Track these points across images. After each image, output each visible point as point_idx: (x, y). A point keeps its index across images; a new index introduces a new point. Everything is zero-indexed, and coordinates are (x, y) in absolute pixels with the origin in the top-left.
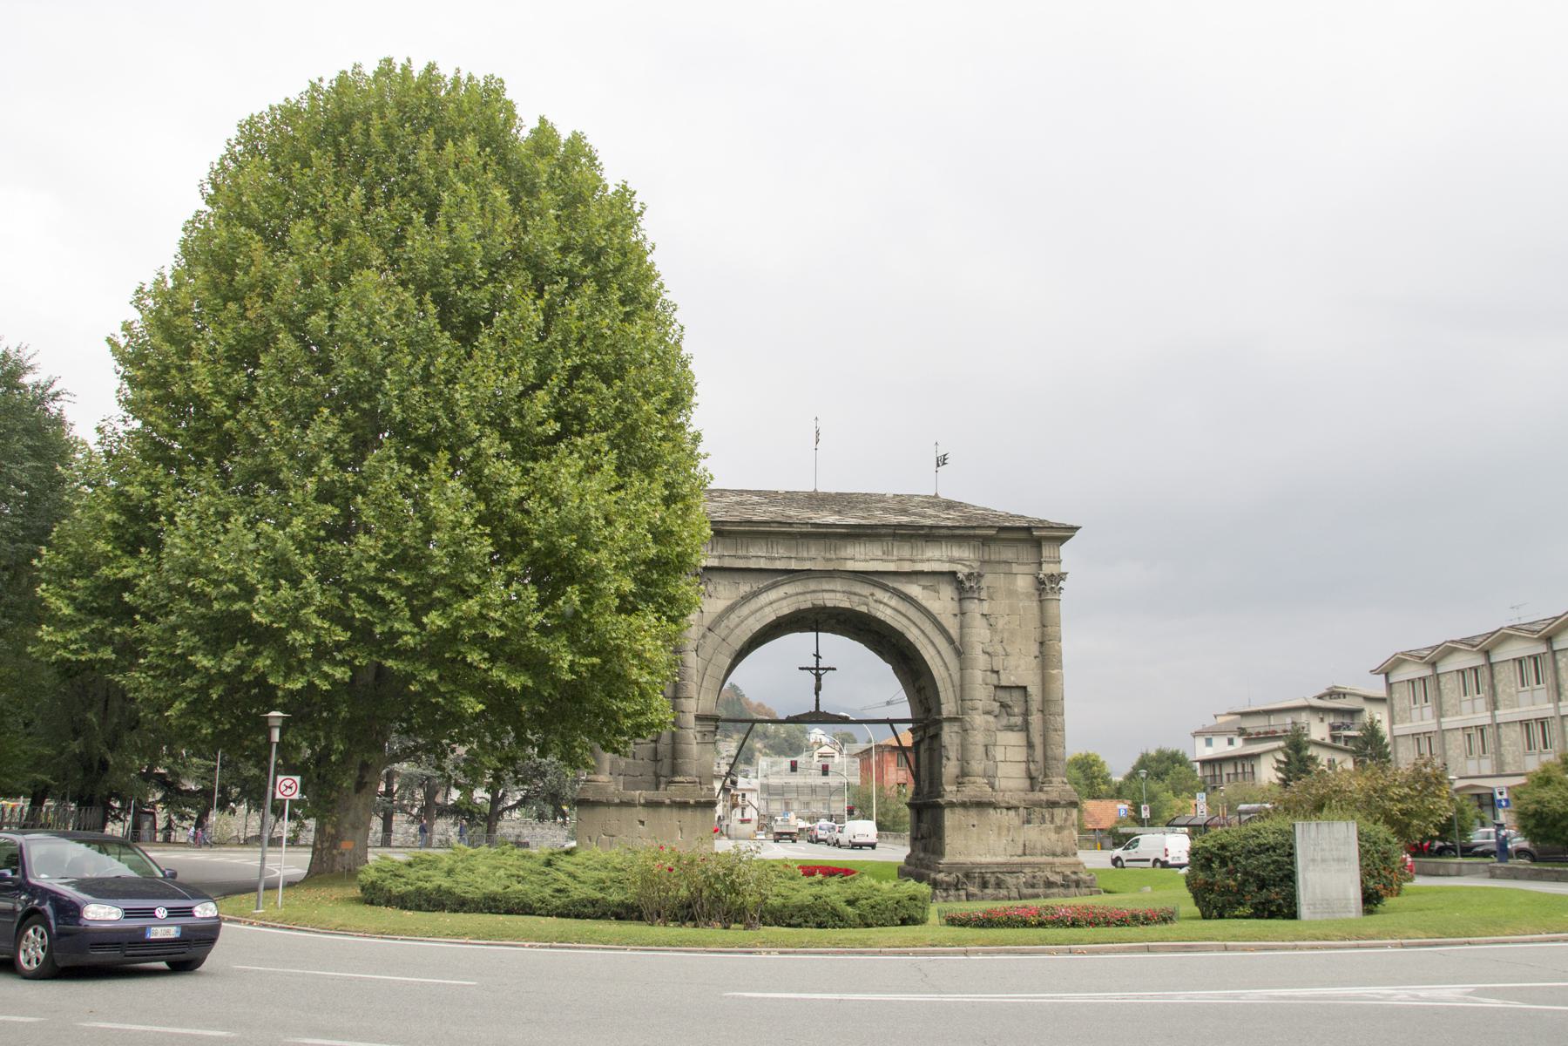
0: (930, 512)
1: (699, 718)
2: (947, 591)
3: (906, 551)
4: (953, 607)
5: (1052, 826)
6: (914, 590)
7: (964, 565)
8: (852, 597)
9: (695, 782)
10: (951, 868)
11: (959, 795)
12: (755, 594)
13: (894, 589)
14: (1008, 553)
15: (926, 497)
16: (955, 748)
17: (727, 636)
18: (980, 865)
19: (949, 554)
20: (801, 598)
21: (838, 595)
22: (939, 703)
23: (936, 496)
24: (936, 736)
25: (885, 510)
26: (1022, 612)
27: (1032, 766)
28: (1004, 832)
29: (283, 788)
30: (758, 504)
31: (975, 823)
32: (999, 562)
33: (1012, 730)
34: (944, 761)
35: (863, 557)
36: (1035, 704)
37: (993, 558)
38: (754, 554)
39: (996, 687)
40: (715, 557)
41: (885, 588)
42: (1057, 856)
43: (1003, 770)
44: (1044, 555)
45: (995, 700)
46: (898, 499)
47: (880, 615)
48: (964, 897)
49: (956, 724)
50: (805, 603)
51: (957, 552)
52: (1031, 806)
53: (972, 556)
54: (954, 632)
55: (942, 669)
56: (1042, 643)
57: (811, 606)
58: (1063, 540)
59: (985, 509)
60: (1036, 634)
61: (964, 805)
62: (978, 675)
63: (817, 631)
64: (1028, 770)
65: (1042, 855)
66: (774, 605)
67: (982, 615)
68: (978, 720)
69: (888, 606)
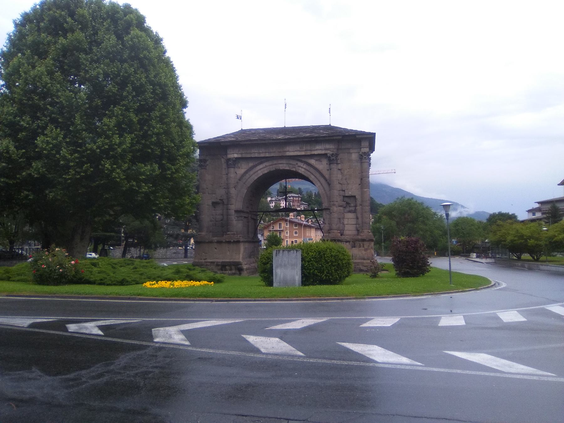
1: (237, 211)
2: (325, 162)
3: (309, 148)
5: (363, 248)
6: (312, 161)
7: (331, 151)
9: (234, 234)
13: (305, 161)
14: (349, 146)
19: (325, 147)
20: (271, 167)
21: (284, 165)
23: (330, 125)
32: (345, 149)
33: (351, 213)
35: (292, 150)
36: (359, 202)
37: (343, 147)
38: (253, 152)
39: (344, 197)
41: (301, 161)
42: (365, 260)
43: (347, 227)
44: (362, 145)
45: (344, 202)
47: (299, 171)
49: (329, 211)
50: (273, 168)
51: (328, 146)
53: (333, 147)
54: (327, 176)
56: (361, 179)
57: (275, 169)
62: (336, 193)
64: (356, 228)
65: (359, 259)
66: (262, 170)
67: (338, 169)
68: (335, 209)
69: (303, 168)
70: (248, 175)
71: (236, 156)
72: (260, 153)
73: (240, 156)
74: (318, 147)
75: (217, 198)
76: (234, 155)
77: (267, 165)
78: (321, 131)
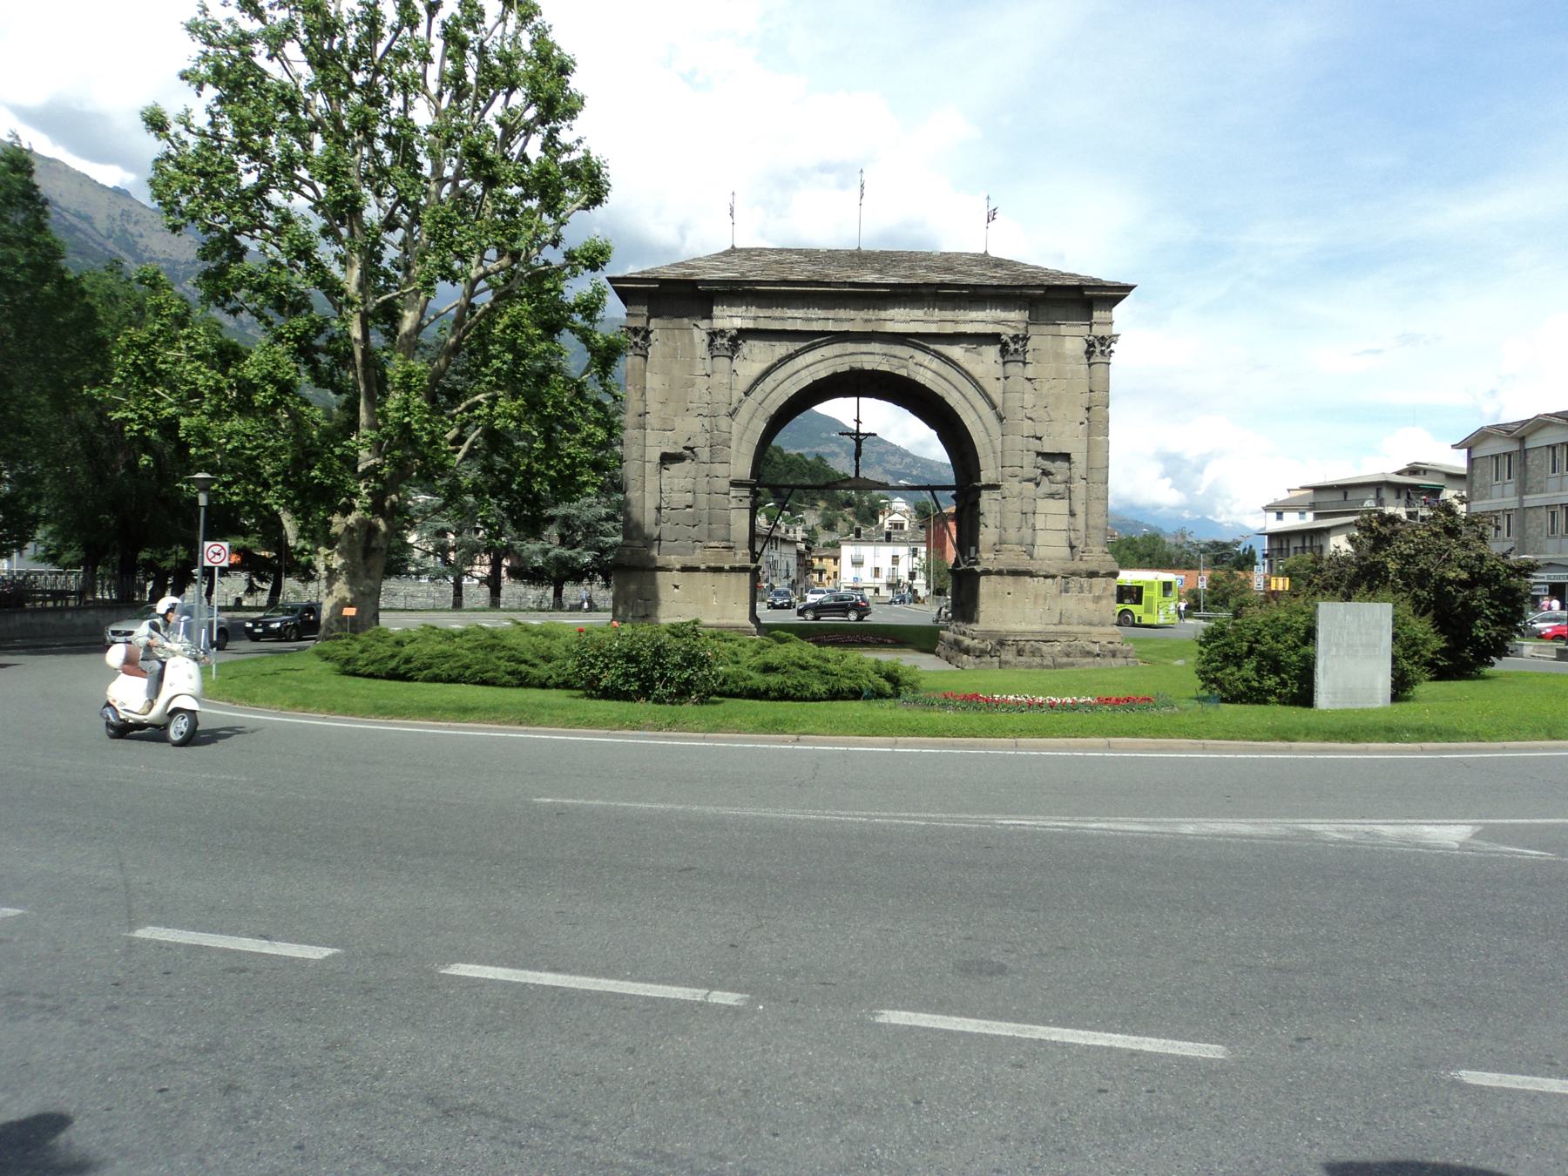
0: (976, 270)
3: (948, 315)
4: (998, 370)
6: (956, 352)
8: (892, 359)
10: (988, 634)
11: (995, 563)
12: (790, 357)
13: (935, 351)
15: (974, 255)
16: (993, 515)
17: (763, 401)
18: (1015, 633)
20: (838, 360)
22: (979, 471)
24: (976, 504)
25: (928, 268)
26: (1069, 376)
27: (1072, 535)
28: (1041, 601)
29: (211, 555)
30: (797, 262)
31: (1011, 591)
34: (982, 528)
35: (903, 318)
38: (790, 315)
39: (1039, 454)
40: (750, 318)
41: (926, 350)
46: (946, 256)
47: (920, 379)
48: (997, 665)
50: (842, 366)
51: (999, 314)
52: (1069, 575)
54: (997, 398)
55: (983, 435)
58: (1116, 300)
59: (1037, 268)
60: (1084, 400)
61: (1000, 573)
63: (858, 396)
65: (1079, 624)
70: (770, 382)
71: (738, 323)
72: (809, 320)
73: (750, 324)
74: (973, 315)
75: (675, 443)
76: (730, 318)
77: (827, 355)
78: (976, 270)
